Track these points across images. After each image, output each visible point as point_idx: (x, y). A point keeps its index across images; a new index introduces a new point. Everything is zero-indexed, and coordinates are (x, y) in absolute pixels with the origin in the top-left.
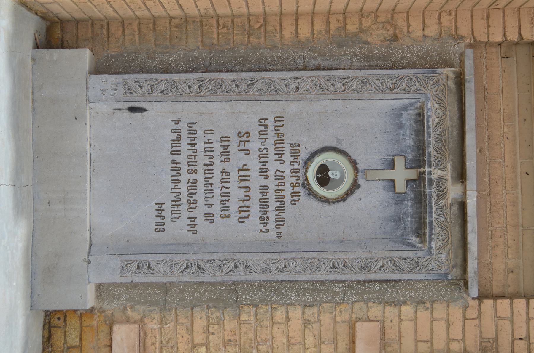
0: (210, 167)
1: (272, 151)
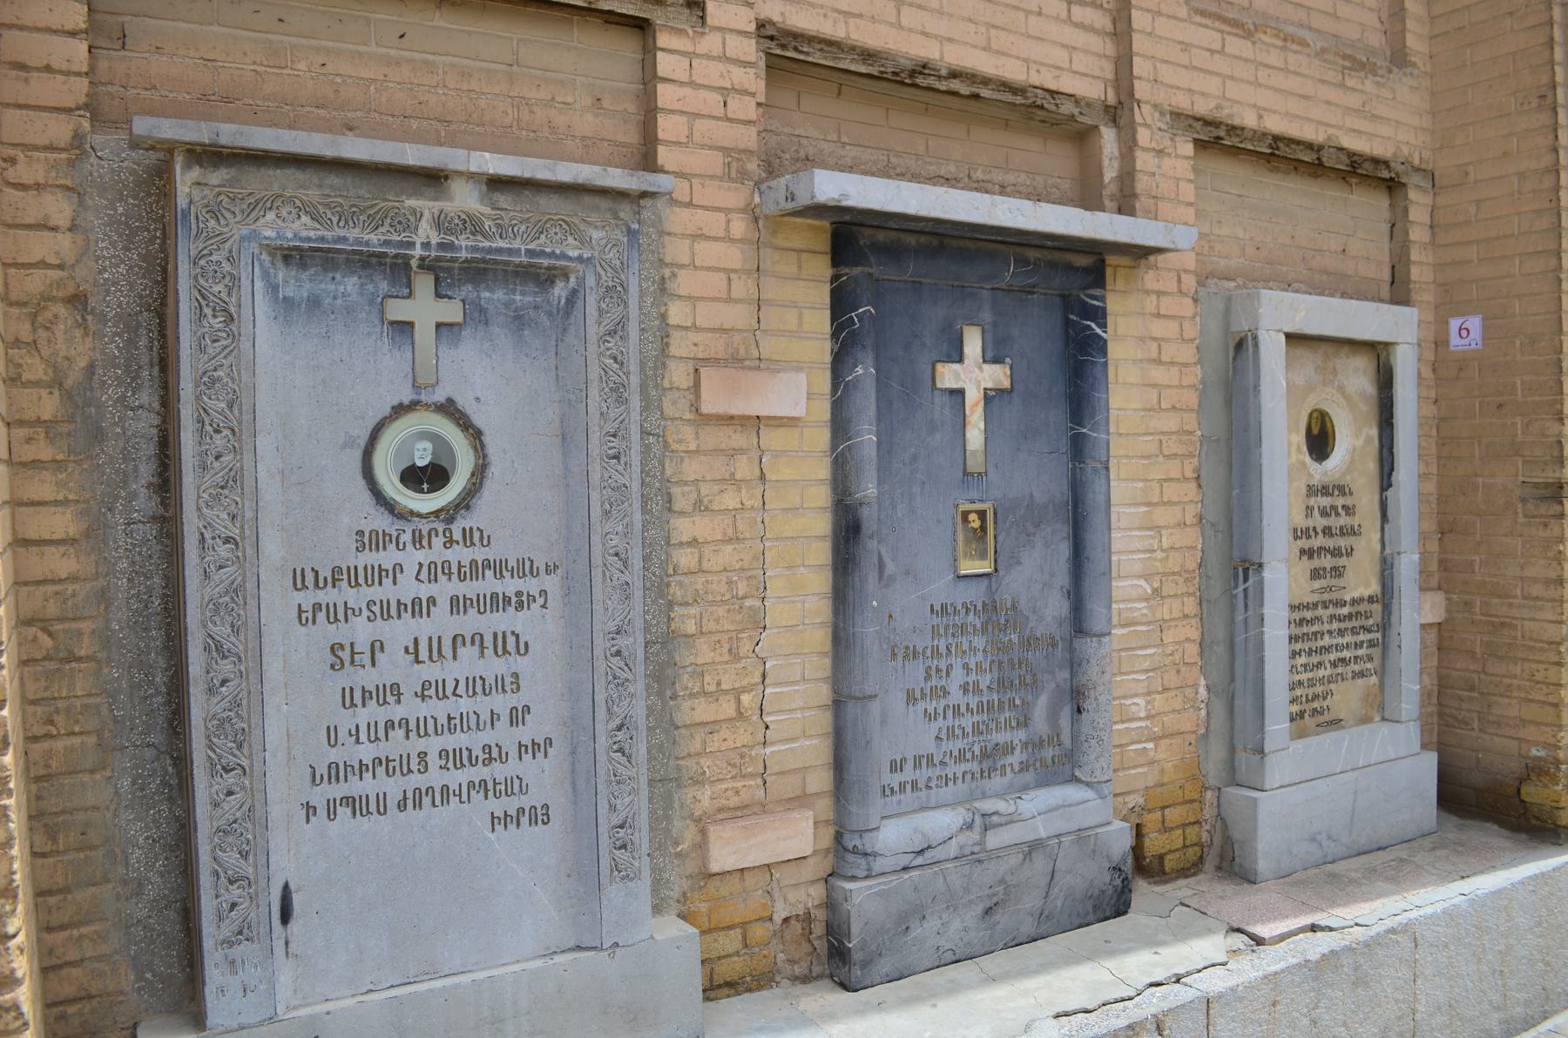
0: (412, 725)
1: (375, 593)
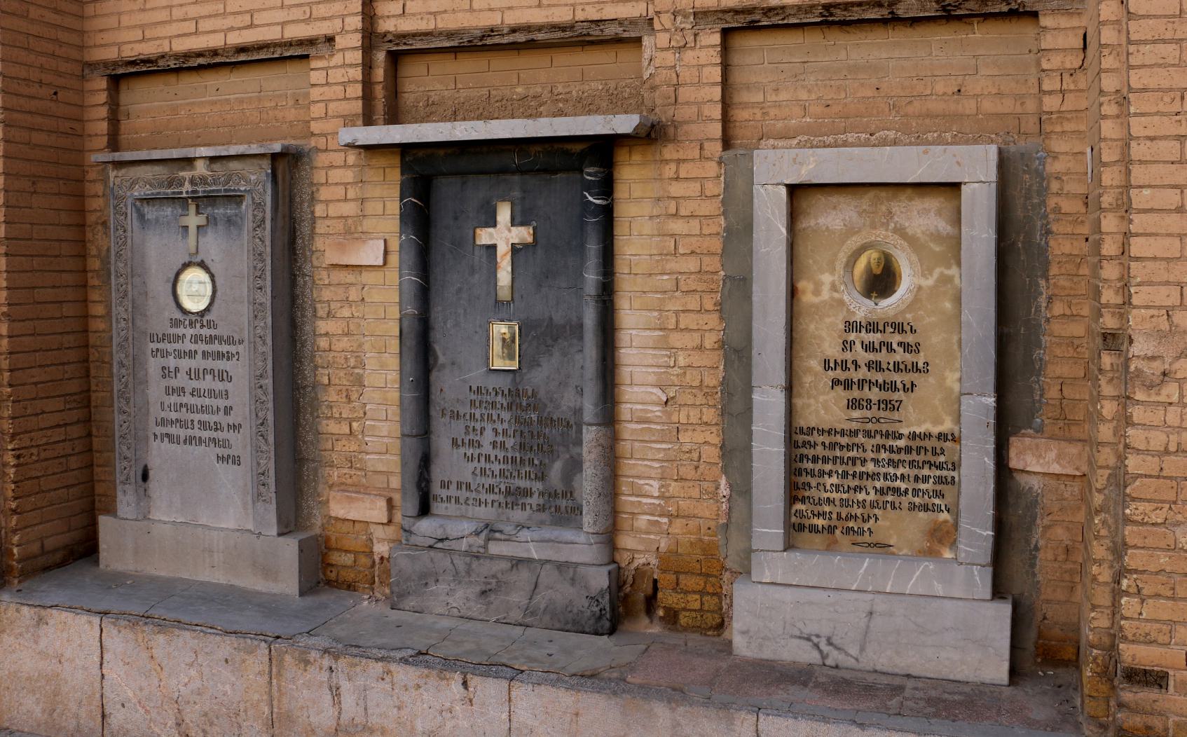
1: (177, 346)
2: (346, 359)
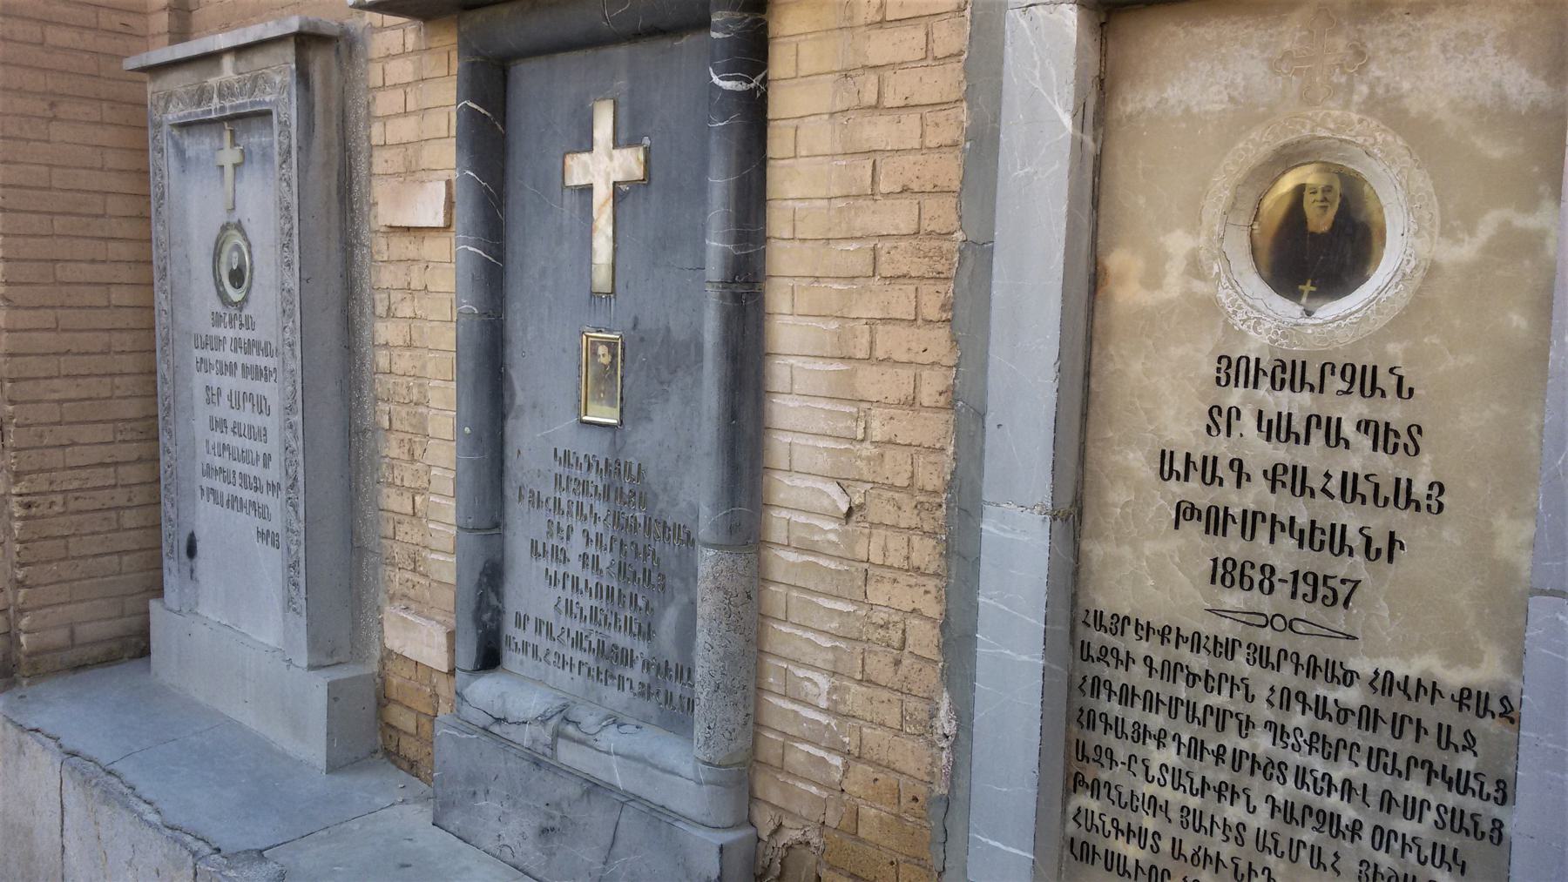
2: (408, 388)
